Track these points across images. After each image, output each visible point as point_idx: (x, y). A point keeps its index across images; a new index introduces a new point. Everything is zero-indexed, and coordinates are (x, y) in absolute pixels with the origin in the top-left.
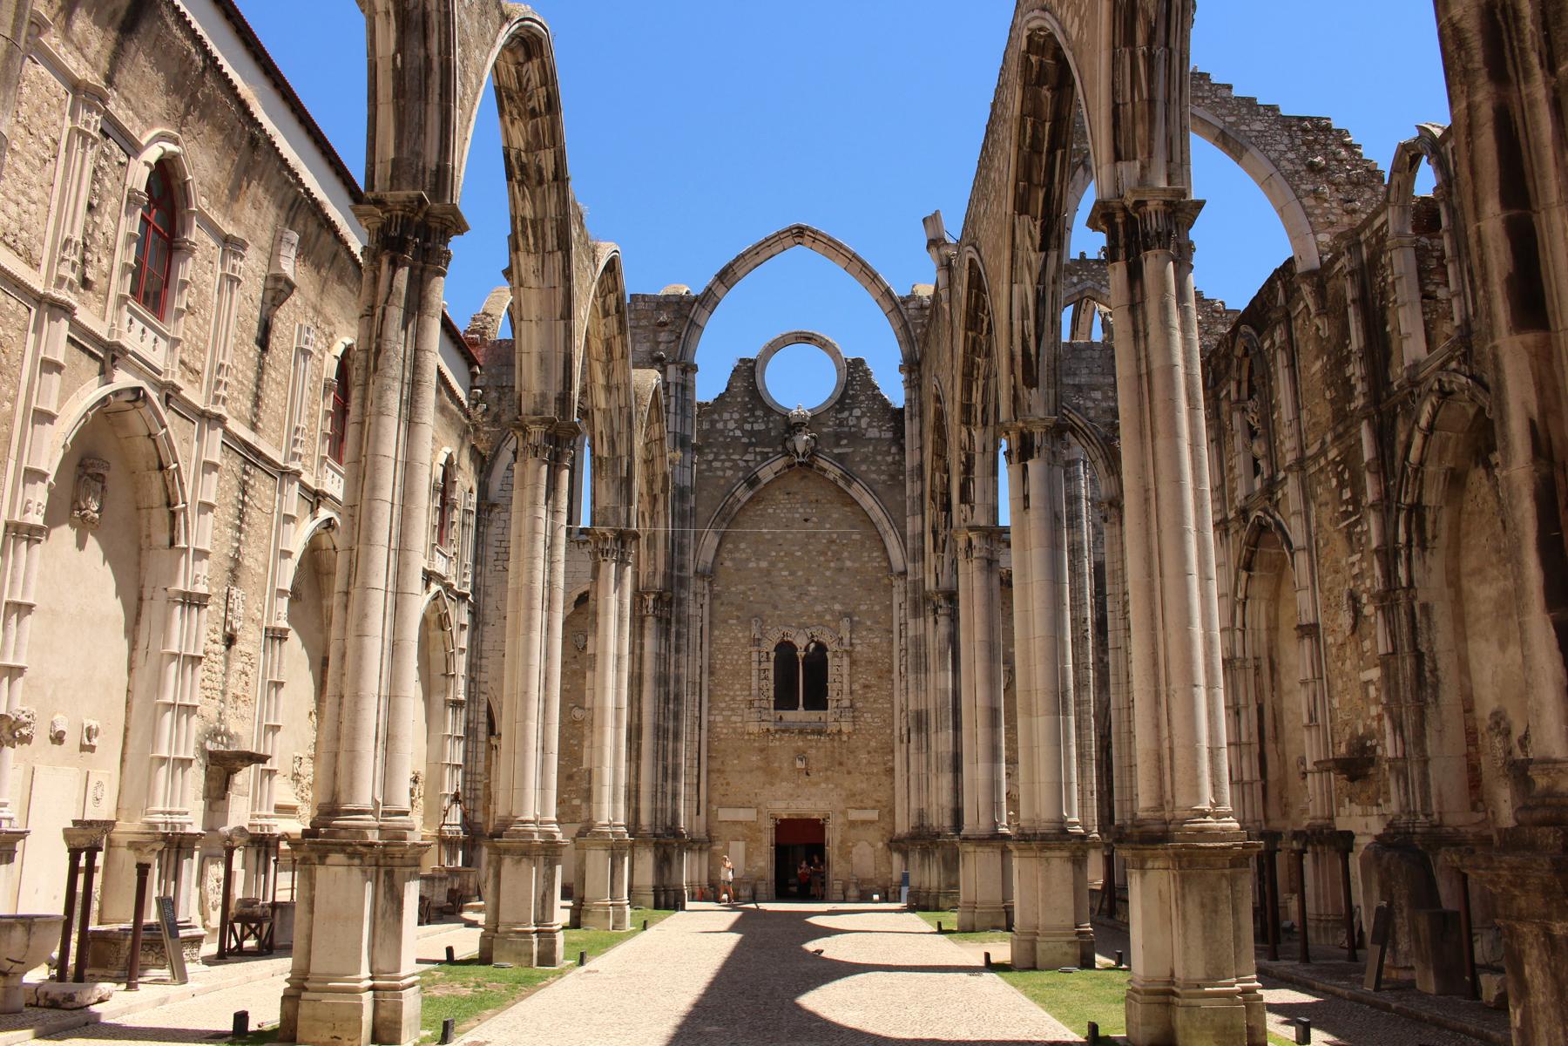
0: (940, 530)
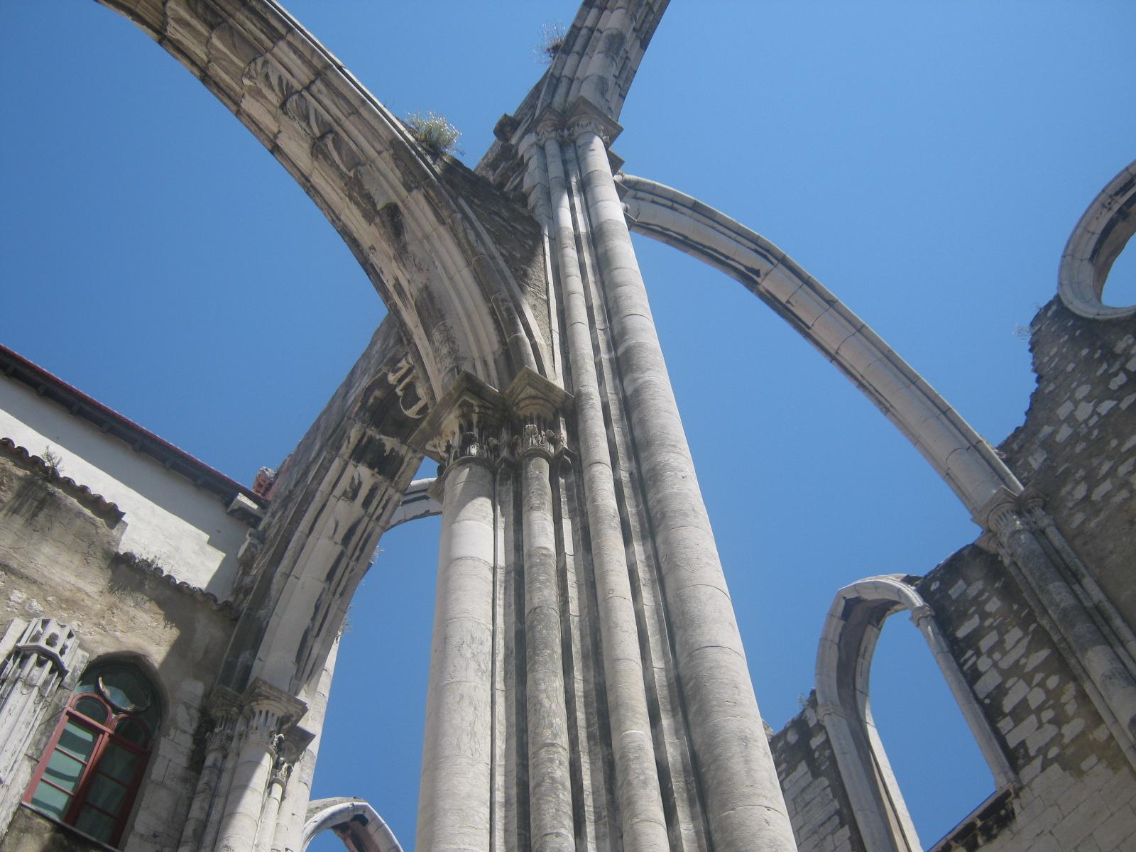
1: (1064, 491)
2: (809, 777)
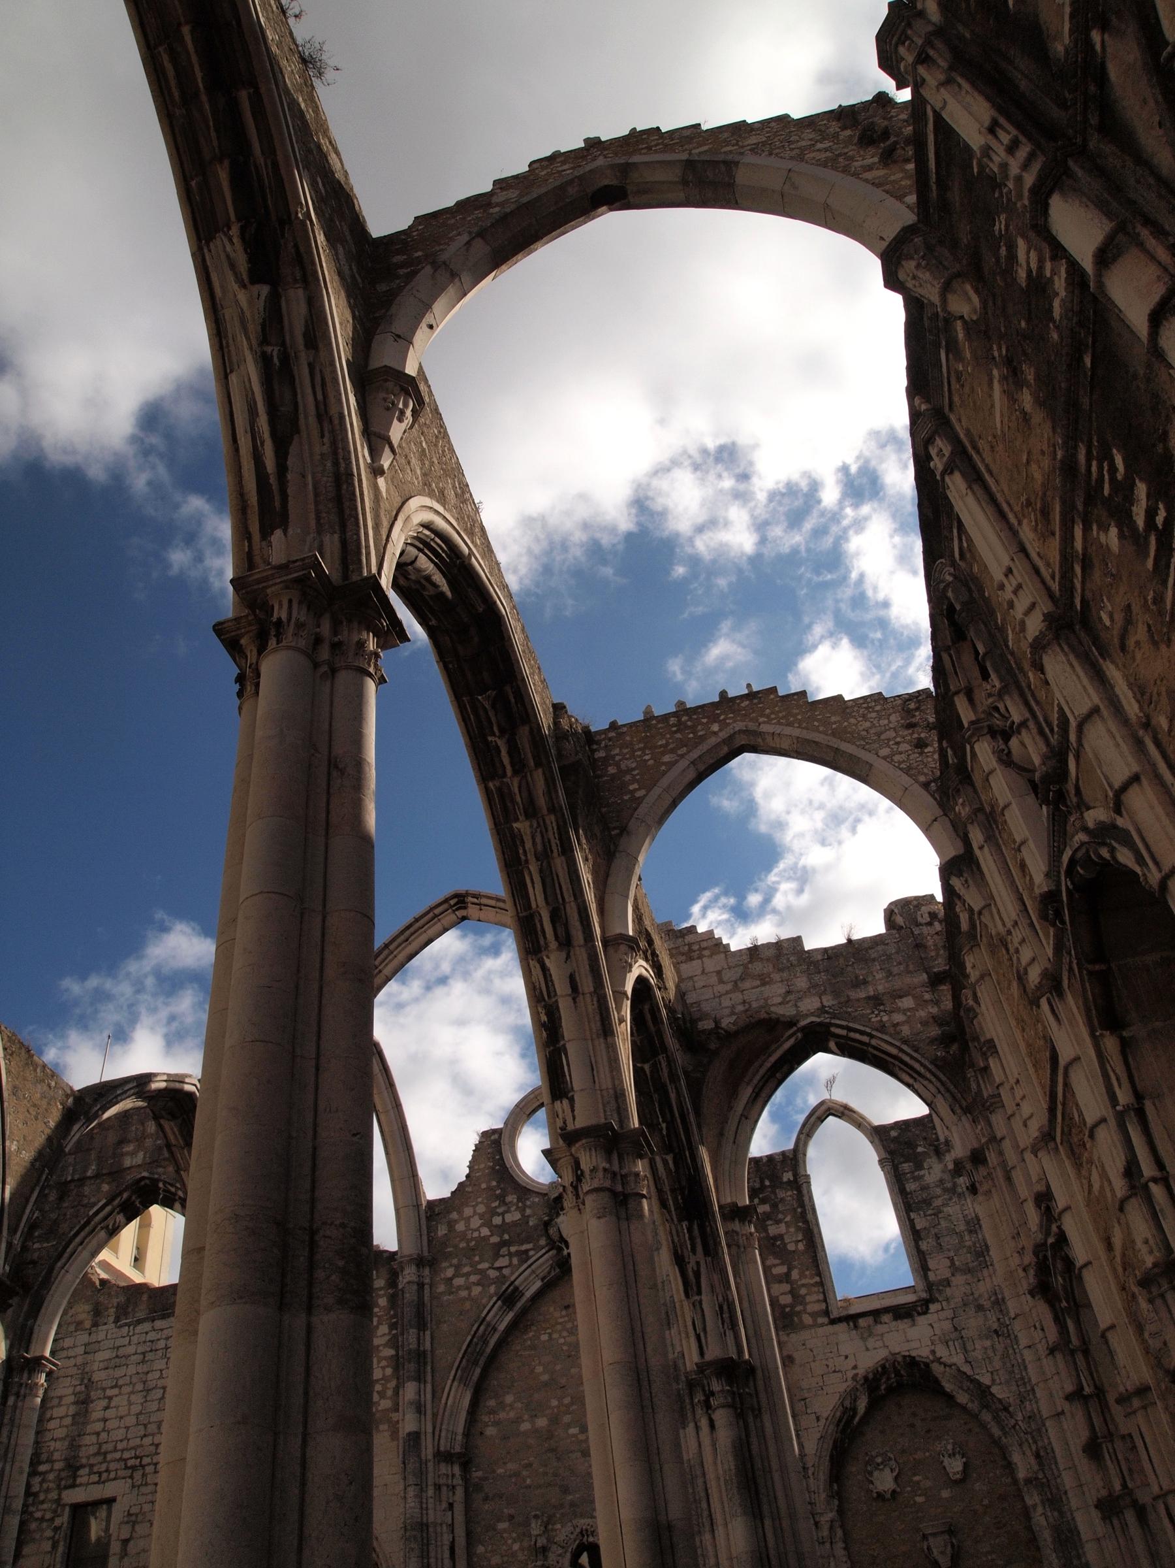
0: (687, 1253)
1: (444, 1264)
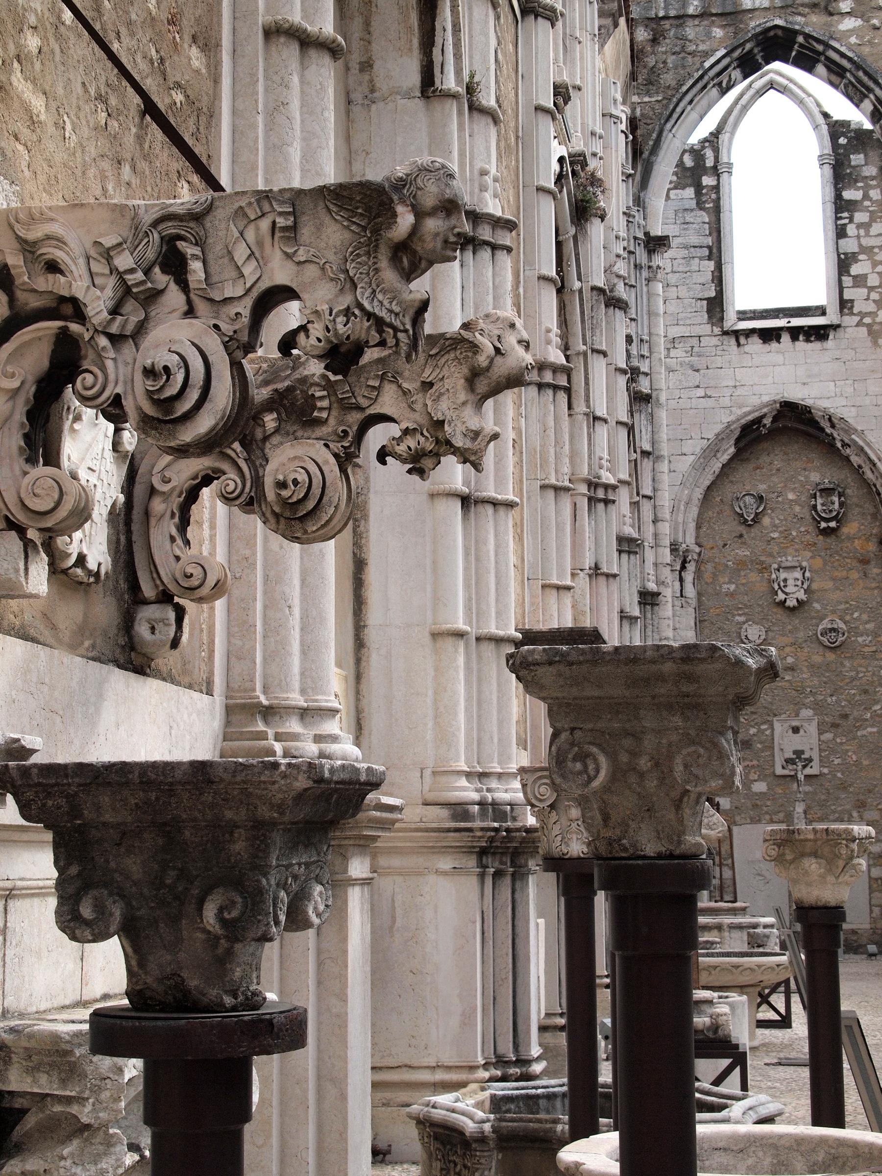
2: (693, 204)
